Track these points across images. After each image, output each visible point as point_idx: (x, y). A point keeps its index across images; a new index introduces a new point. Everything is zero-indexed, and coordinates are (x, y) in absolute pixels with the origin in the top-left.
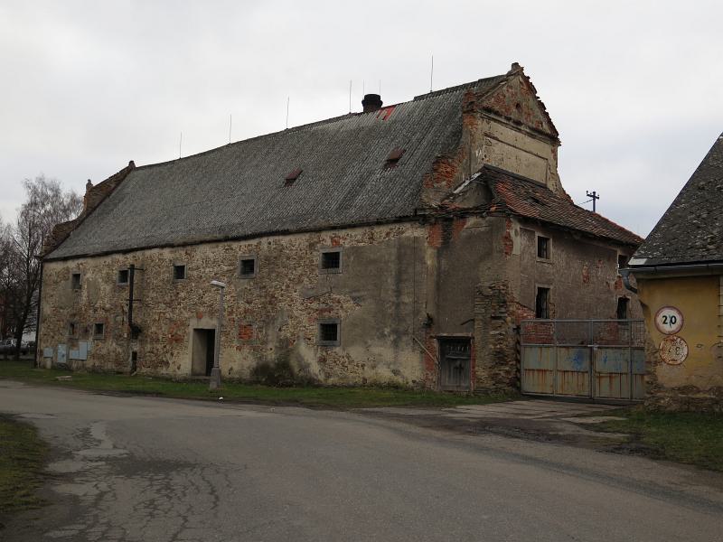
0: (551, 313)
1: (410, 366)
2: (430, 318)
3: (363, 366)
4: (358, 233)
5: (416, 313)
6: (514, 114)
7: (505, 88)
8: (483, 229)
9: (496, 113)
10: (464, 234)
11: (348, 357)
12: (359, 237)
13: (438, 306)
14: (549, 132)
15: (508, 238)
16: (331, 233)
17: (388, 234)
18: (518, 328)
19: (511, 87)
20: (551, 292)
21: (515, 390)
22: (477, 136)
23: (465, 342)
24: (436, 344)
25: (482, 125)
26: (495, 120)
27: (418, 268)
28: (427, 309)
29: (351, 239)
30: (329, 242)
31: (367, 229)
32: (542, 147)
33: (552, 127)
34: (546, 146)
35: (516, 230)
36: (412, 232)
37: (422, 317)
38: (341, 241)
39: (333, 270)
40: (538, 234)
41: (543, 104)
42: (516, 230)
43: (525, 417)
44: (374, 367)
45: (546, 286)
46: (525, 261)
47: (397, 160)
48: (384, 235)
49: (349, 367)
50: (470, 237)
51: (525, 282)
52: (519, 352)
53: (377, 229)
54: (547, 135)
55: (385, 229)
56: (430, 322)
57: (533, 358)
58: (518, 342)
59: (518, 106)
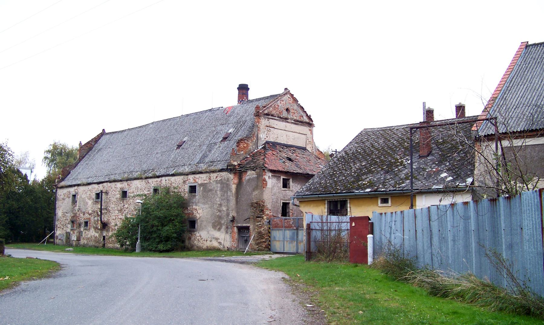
0: (291, 214)
1: (118, 245)
2: (234, 217)
3: (207, 240)
4: (204, 176)
5: (228, 215)
6: (285, 114)
7: (279, 102)
8: (254, 176)
9: (272, 115)
10: (247, 178)
11: (200, 236)
12: (205, 178)
13: (237, 212)
14: (307, 121)
15: (265, 180)
16: (193, 176)
17: (217, 177)
18: (270, 221)
19: (283, 101)
20: (291, 204)
21: (268, 249)
22: (261, 128)
23: (247, 228)
24: (236, 229)
25: (264, 122)
26: (273, 119)
27: (229, 193)
28: (233, 214)
29: (201, 179)
30: (192, 181)
31: (208, 174)
32: (305, 129)
33: (309, 117)
34: (305, 127)
35: (269, 177)
36: (225, 175)
37: (230, 218)
38: (197, 180)
39: (194, 194)
40: (282, 177)
41: (302, 107)
42: (269, 177)
43: (209, 258)
44: (211, 241)
45: (288, 202)
46: (275, 190)
47: (227, 138)
48: (215, 177)
49: (201, 241)
50: (249, 180)
51: (274, 200)
52: (270, 233)
53: (212, 175)
54: (306, 123)
55: (215, 175)
56: (233, 220)
57: (277, 234)
58: (270, 228)
59: (287, 110)
